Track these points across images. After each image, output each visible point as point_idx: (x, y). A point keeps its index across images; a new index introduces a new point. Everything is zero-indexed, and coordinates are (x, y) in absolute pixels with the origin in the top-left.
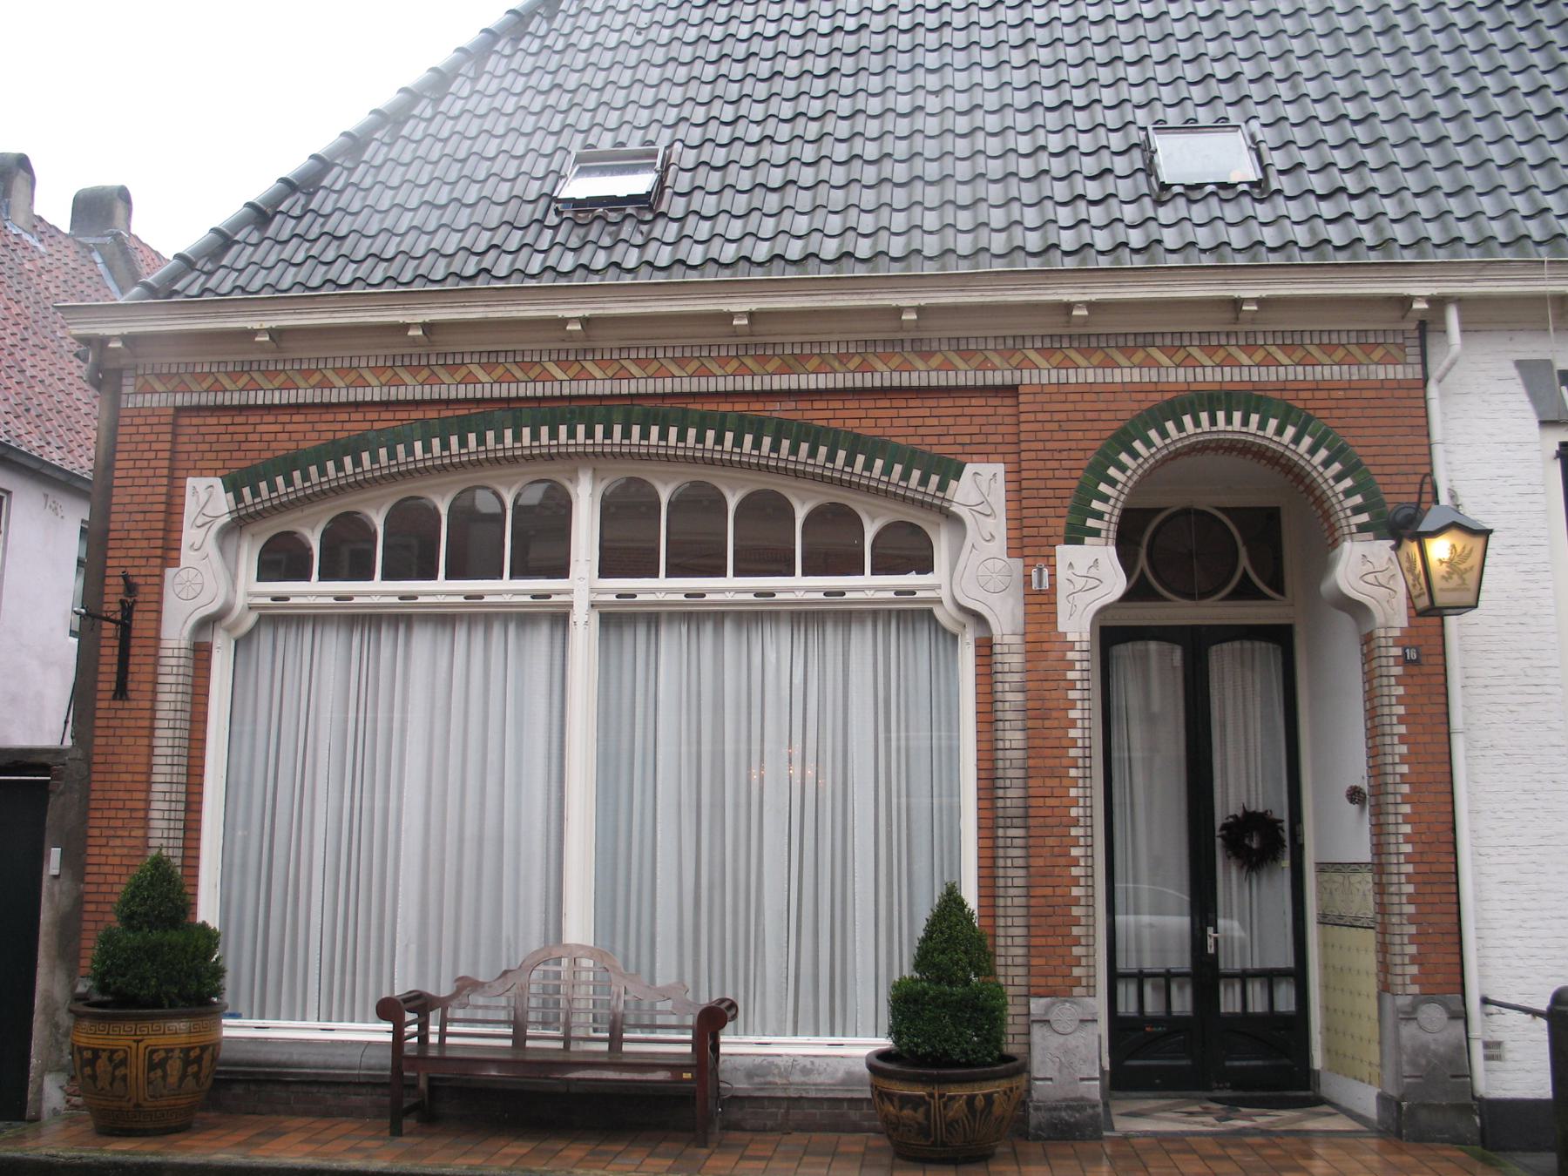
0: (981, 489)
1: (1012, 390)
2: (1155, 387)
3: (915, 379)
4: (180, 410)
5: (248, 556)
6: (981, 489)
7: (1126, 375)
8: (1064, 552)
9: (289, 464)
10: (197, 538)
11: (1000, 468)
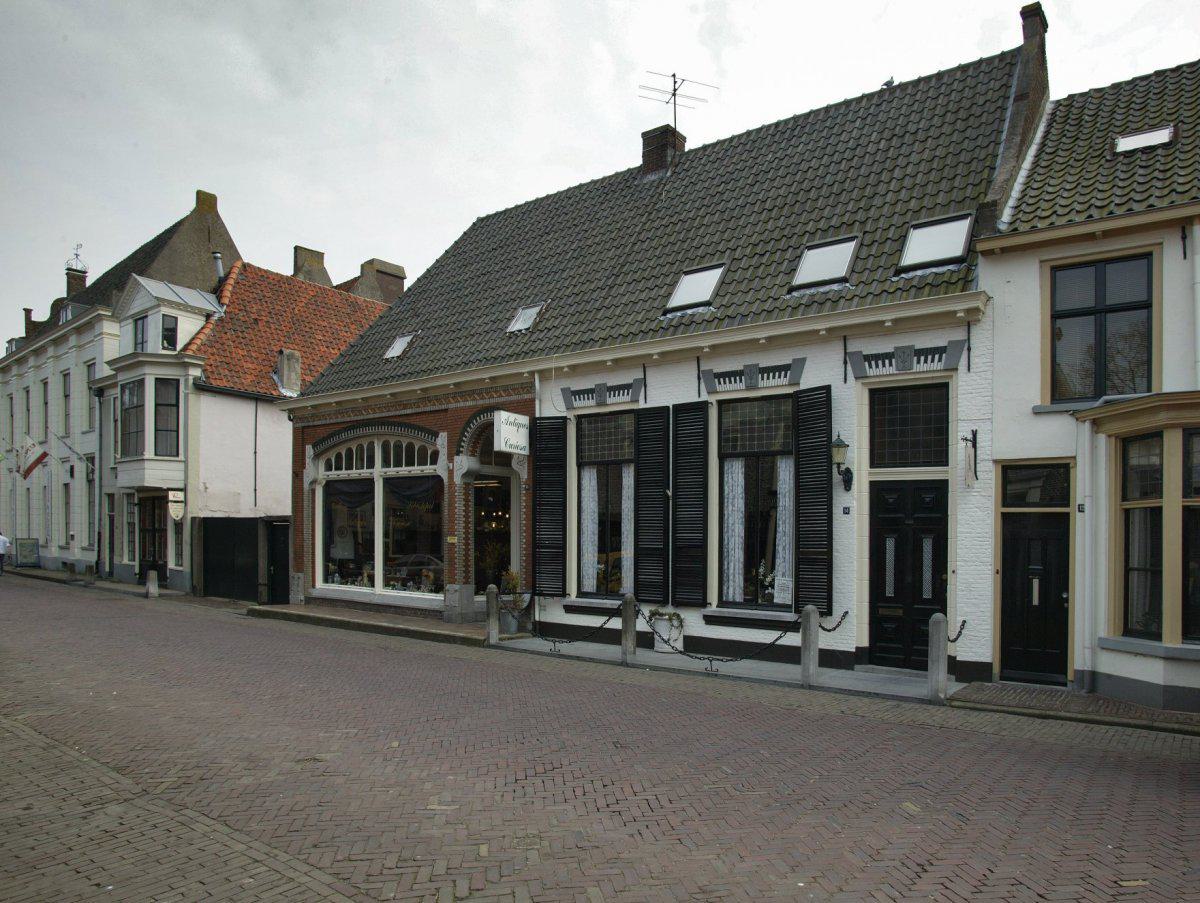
0: (442, 440)
1: (446, 410)
2: (475, 407)
3: (428, 409)
4: (304, 427)
6: (442, 440)
7: (470, 403)
8: (456, 458)
9: (324, 440)
11: (446, 433)
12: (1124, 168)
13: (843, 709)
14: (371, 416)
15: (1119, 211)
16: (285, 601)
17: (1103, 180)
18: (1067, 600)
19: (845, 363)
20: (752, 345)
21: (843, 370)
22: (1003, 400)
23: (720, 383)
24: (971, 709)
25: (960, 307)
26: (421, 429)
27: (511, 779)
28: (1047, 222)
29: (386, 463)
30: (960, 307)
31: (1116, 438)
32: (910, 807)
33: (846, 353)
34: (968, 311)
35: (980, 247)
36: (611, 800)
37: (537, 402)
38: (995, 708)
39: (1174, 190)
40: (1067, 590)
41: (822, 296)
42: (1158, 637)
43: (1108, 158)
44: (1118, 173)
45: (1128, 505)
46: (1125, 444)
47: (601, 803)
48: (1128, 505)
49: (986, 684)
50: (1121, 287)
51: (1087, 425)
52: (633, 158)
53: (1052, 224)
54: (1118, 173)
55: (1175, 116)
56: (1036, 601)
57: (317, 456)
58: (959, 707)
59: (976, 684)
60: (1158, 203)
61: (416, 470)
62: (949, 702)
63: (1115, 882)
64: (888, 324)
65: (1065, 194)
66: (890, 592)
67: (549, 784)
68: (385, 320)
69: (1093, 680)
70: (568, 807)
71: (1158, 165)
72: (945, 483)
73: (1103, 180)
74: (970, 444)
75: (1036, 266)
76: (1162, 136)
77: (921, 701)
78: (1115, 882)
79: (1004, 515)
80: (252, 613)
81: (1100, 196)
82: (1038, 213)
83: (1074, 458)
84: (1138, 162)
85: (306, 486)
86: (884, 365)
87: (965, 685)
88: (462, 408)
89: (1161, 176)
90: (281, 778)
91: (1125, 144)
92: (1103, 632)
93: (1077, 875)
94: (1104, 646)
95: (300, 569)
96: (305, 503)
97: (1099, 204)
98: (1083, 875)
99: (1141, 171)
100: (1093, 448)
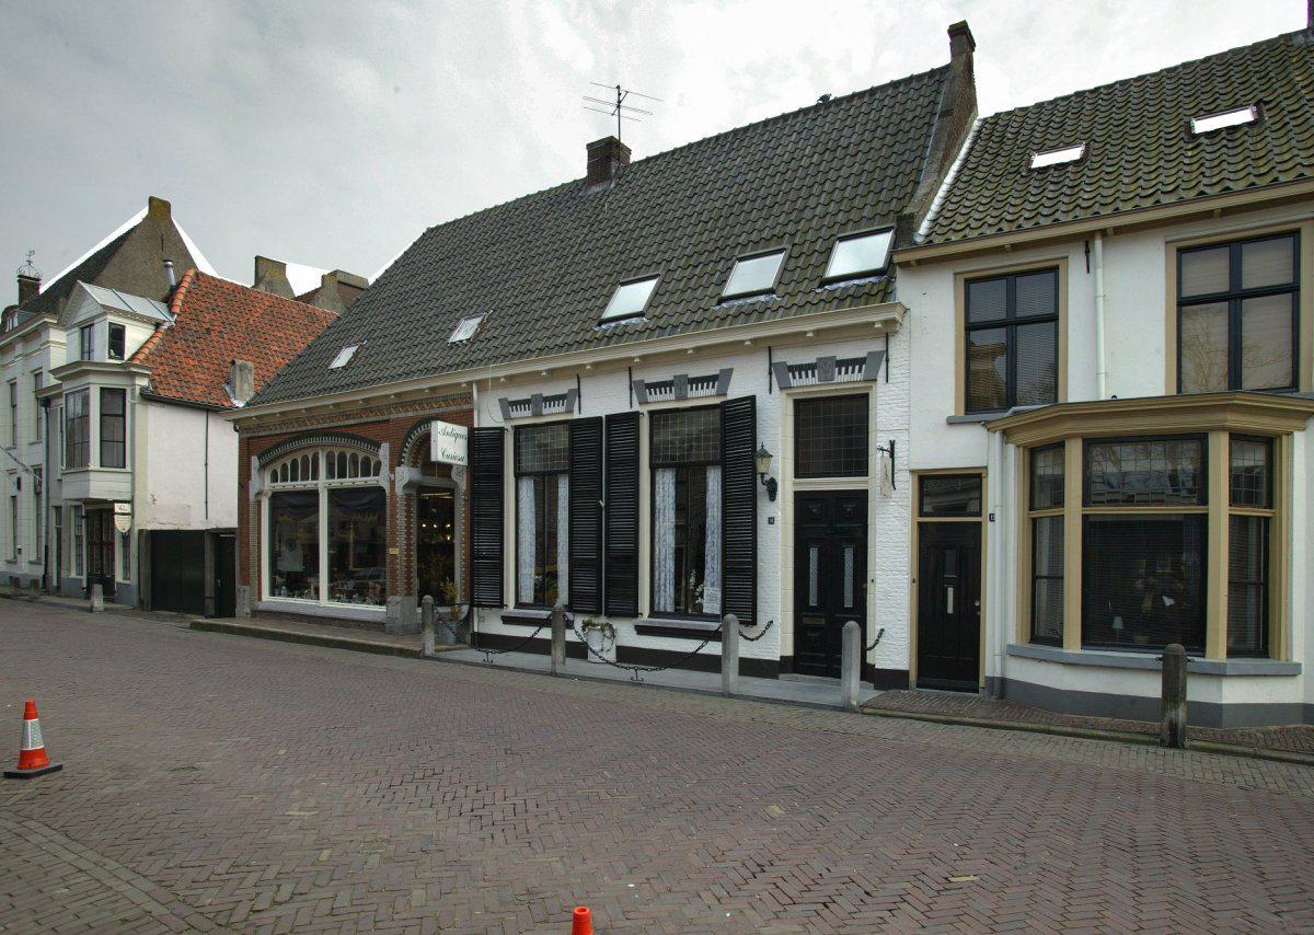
0: (384, 451)
3: (370, 419)
4: (249, 438)
5: (268, 477)
6: (384, 451)
7: (411, 414)
8: (398, 469)
9: (269, 451)
10: (254, 472)
12: (1037, 184)
13: (755, 715)
14: (314, 427)
15: (1027, 225)
16: (232, 615)
17: (1016, 194)
18: (979, 608)
19: (770, 373)
20: (534, 377)
21: (768, 380)
22: (919, 413)
23: (651, 394)
24: (881, 715)
25: (877, 318)
26: (363, 439)
27: (385, 784)
28: (961, 234)
29: (331, 474)
30: (877, 318)
31: (1025, 448)
32: (776, 810)
33: (770, 364)
34: (886, 322)
35: (896, 259)
36: (478, 804)
37: (476, 413)
38: (903, 714)
39: (1078, 205)
40: (979, 599)
41: (751, 307)
42: (1059, 643)
43: (1023, 174)
44: (1030, 189)
45: (1035, 514)
46: (1033, 453)
47: (466, 808)
48: (1035, 514)
49: (902, 691)
50: (1031, 300)
51: (998, 435)
52: (578, 169)
53: (965, 236)
54: (1030, 189)
55: (1088, 135)
56: (950, 610)
57: (263, 467)
58: (870, 714)
59: (892, 692)
60: (1063, 218)
61: (360, 481)
62: (862, 710)
63: (946, 879)
64: (810, 335)
65: (981, 208)
66: (813, 601)
67: (422, 789)
68: (332, 330)
69: (1002, 686)
70: (431, 812)
71: (1067, 181)
72: (865, 492)
73: (1016, 194)
74: (887, 454)
75: (952, 275)
76: (1074, 154)
77: (835, 708)
78: (946, 879)
79: (919, 523)
80: (196, 626)
81: (1011, 210)
82: (953, 226)
83: (986, 468)
84: (1050, 178)
85: (252, 497)
86: (661, 393)
87: (881, 692)
88: (403, 419)
89: (1068, 192)
90: (147, 787)
91: (1040, 161)
92: (1012, 640)
93: (912, 873)
94: (1013, 653)
95: (246, 582)
96: (251, 516)
97: (1009, 217)
98: (917, 872)
99: (1052, 187)
100: (1003, 457)
